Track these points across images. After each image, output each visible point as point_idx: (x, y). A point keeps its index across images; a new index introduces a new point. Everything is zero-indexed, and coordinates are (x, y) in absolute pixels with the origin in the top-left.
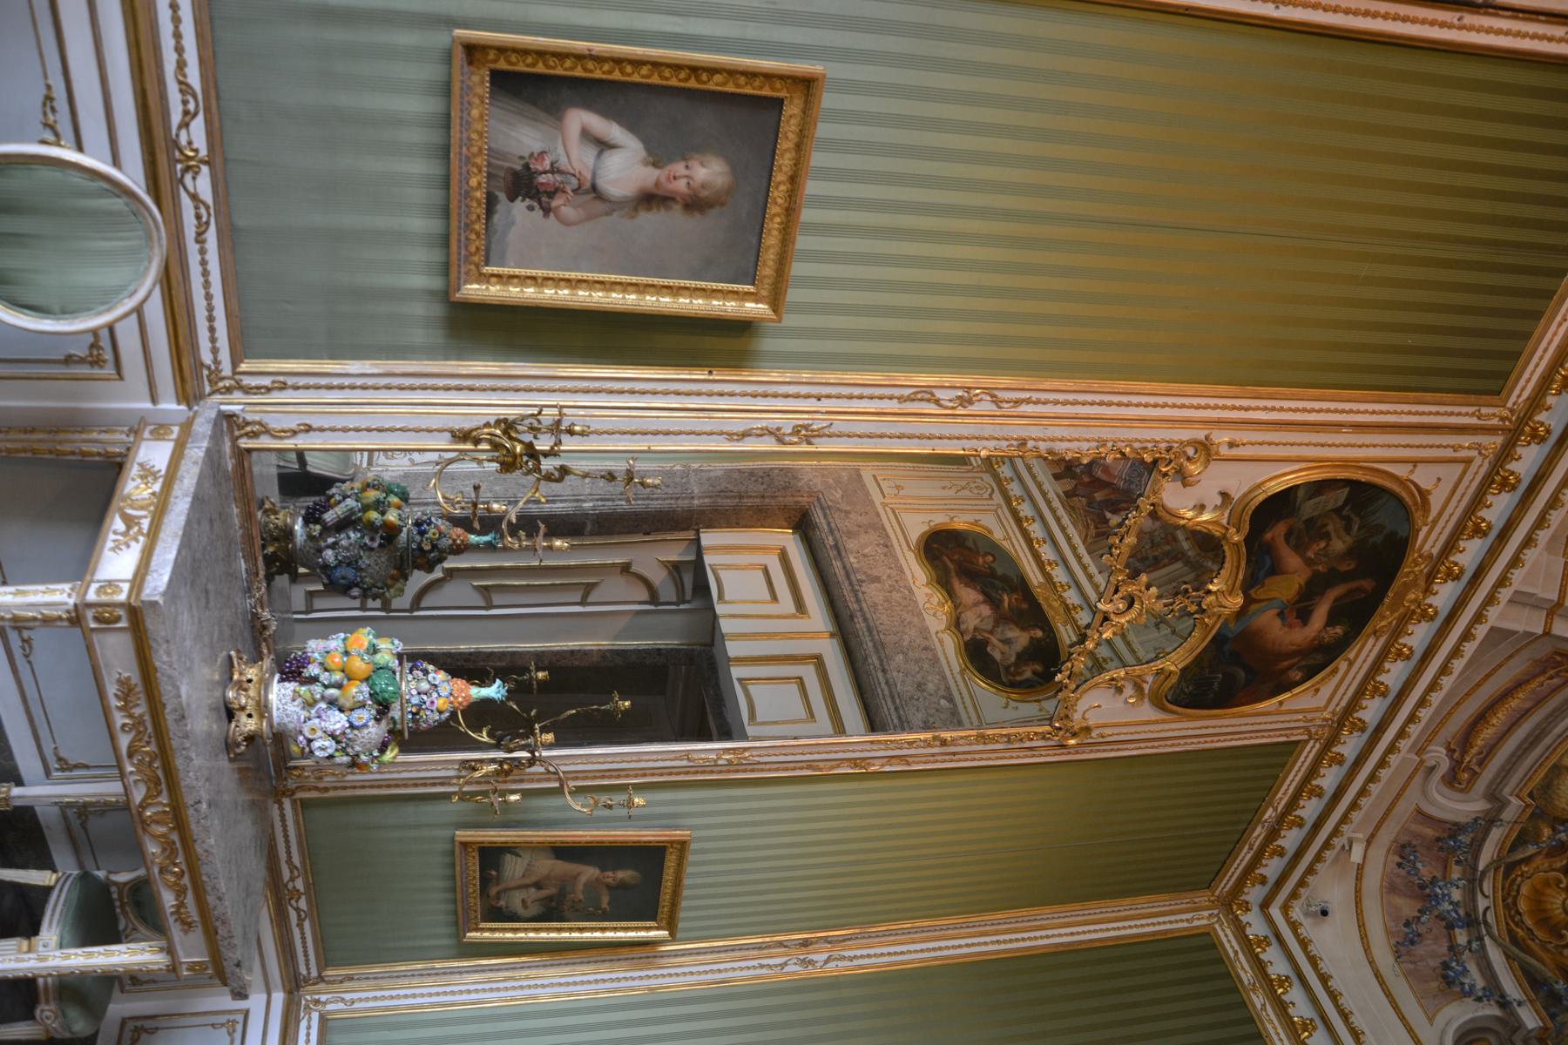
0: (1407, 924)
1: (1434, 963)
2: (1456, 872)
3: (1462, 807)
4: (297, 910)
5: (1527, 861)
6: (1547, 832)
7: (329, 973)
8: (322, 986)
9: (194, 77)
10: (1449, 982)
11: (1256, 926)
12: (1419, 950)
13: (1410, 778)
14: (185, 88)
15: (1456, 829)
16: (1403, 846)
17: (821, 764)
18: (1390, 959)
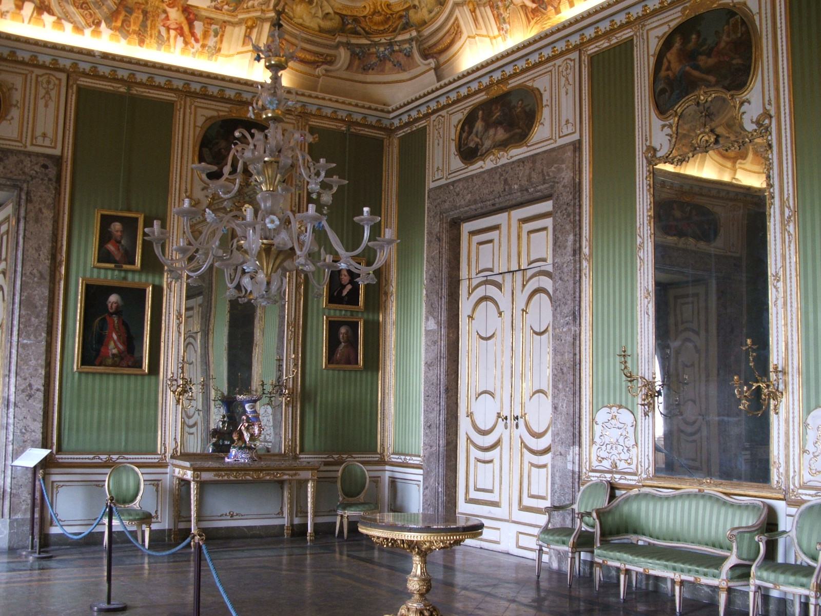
0: (395, 66)
1: (405, 59)
2: (373, 50)
3: (343, 55)
4: (347, 458)
5: (364, 29)
6: (349, 26)
7: (379, 451)
8: (385, 454)
9: (91, 456)
10: (409, 56)
11: (396, 123)
12: (402, 62)
13: (331, 77)
14: (94, 458)
15: (354, 55)
16: (364, 69)
17: (298, 298)
18: (406, 73)
